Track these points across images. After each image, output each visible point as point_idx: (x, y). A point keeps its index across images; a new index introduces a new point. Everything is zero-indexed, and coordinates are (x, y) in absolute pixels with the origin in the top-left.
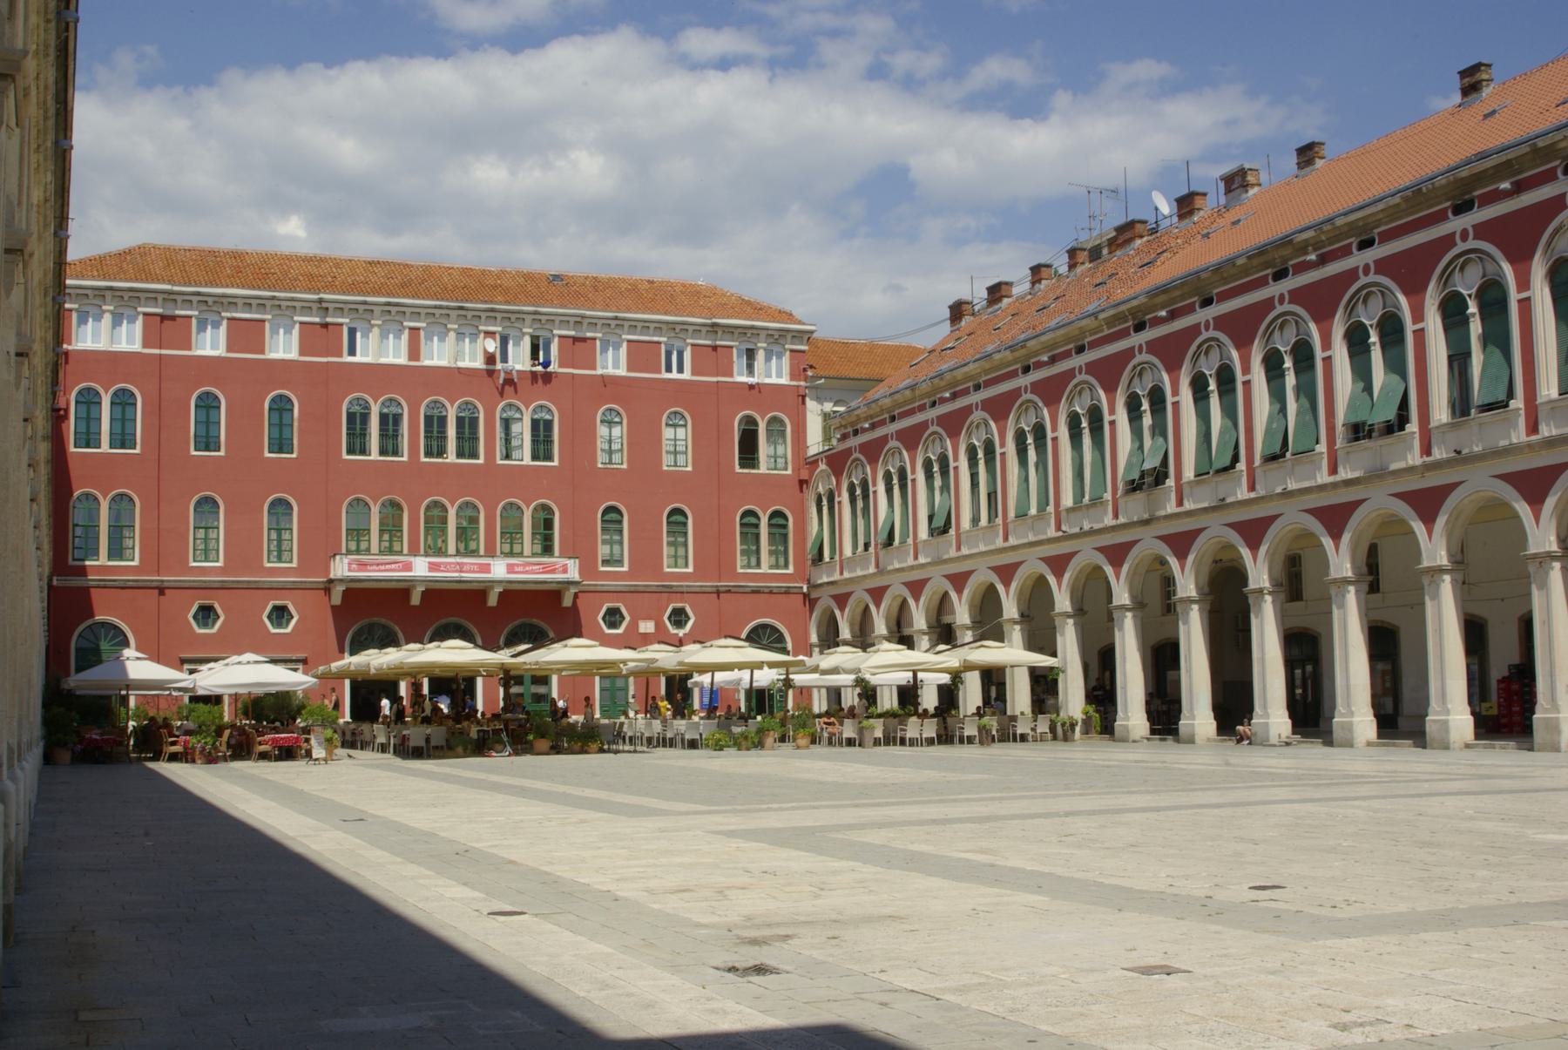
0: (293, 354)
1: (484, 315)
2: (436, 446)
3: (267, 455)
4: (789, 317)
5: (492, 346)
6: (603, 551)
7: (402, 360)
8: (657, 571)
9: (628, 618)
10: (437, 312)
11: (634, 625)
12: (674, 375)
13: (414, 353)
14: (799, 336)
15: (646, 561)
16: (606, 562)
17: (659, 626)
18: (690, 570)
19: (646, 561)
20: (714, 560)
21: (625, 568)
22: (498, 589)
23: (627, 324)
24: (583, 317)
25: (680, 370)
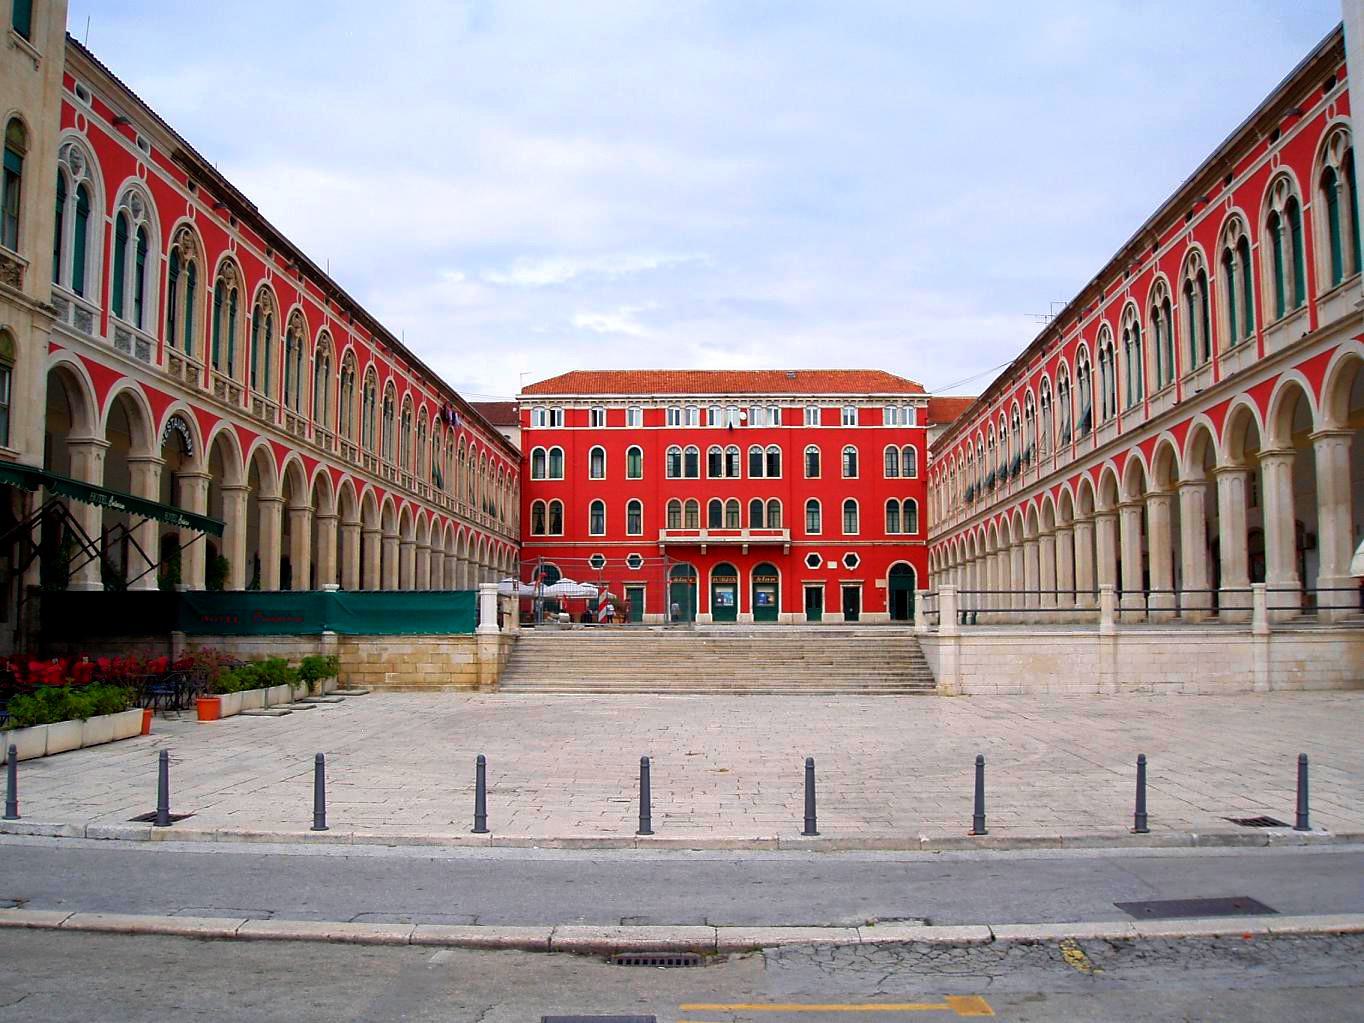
0: (640, 426)
1: (739, 400)
2: (715, 471)
3: (627, 478)
4: (920, 389)
5: (743, 416)
6: (807, 523)
7: (698, 427)
8: (838, 535)
9: (822, 560)
10: (714, 400)
11: (825, 565)
12: (849, 426)
13: (703, 423)
14: (921, 400)
15: (832, 529)
16: (808, 531)
17: (840, 564)
18: (858, 534)
19: (832, 529)
20: (872, 528)
21: (820, 534)
22: (746, 546)
23: (820, 399)
24: (795, 397)
25: (852, 423)
